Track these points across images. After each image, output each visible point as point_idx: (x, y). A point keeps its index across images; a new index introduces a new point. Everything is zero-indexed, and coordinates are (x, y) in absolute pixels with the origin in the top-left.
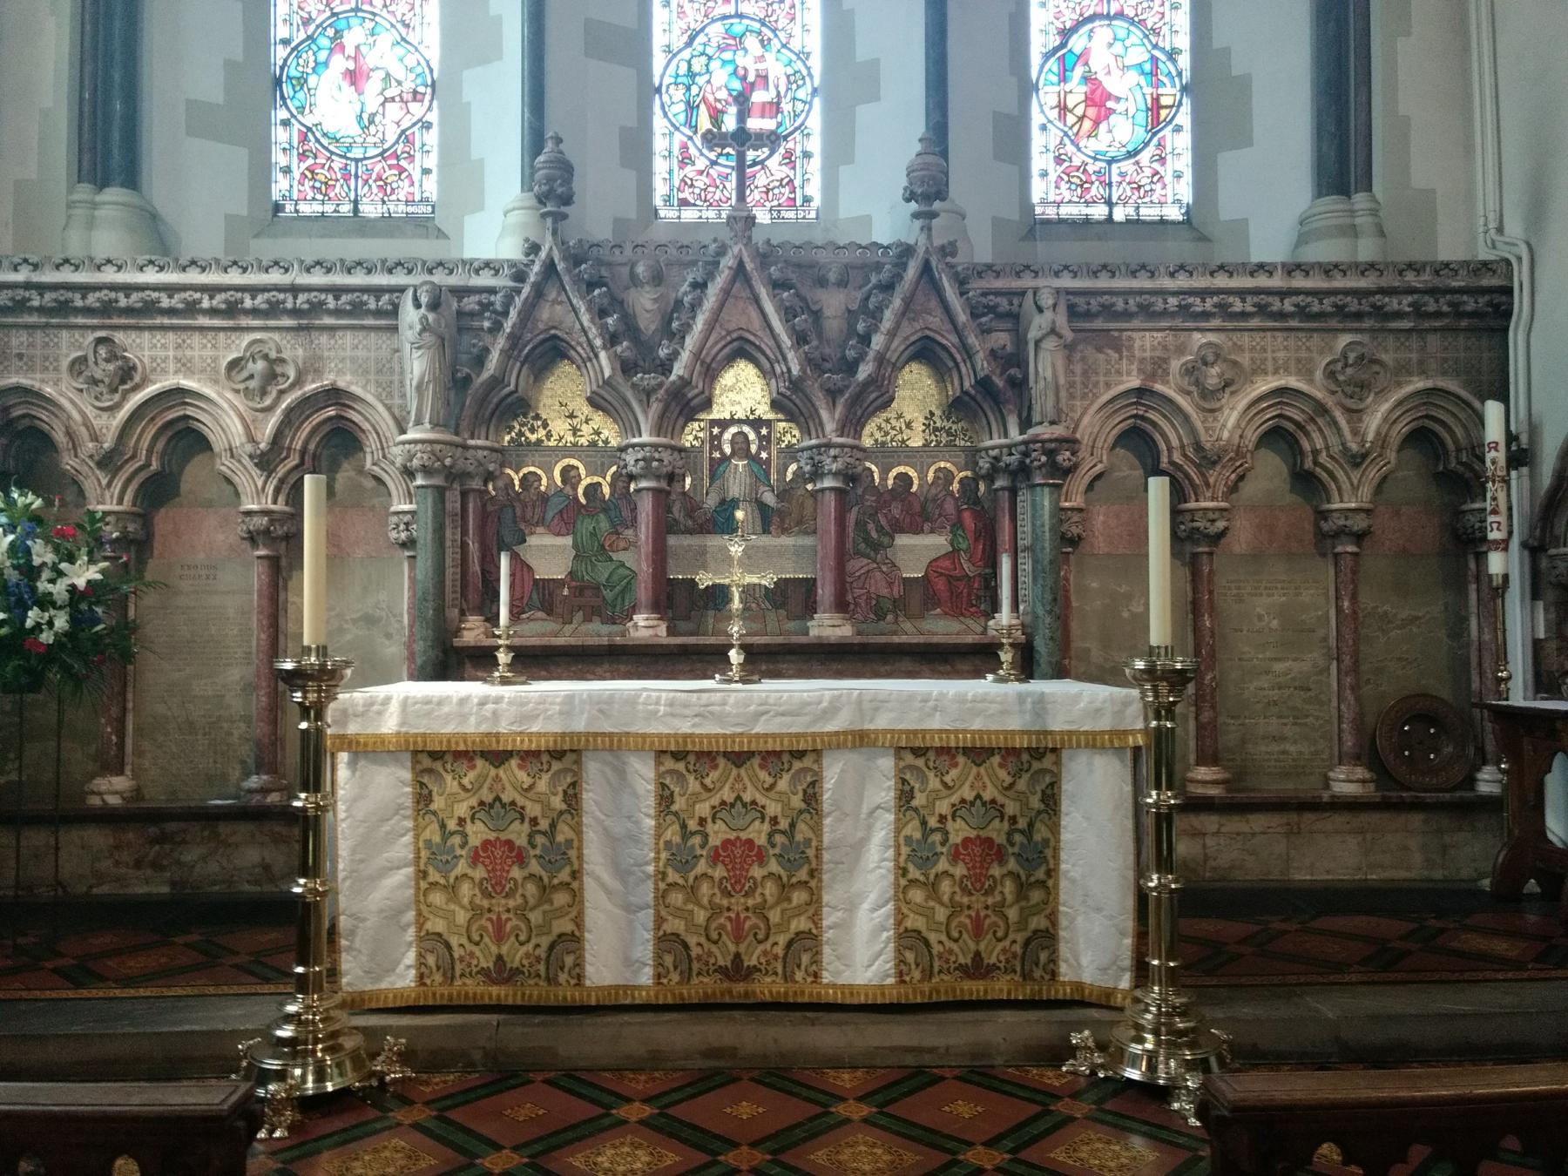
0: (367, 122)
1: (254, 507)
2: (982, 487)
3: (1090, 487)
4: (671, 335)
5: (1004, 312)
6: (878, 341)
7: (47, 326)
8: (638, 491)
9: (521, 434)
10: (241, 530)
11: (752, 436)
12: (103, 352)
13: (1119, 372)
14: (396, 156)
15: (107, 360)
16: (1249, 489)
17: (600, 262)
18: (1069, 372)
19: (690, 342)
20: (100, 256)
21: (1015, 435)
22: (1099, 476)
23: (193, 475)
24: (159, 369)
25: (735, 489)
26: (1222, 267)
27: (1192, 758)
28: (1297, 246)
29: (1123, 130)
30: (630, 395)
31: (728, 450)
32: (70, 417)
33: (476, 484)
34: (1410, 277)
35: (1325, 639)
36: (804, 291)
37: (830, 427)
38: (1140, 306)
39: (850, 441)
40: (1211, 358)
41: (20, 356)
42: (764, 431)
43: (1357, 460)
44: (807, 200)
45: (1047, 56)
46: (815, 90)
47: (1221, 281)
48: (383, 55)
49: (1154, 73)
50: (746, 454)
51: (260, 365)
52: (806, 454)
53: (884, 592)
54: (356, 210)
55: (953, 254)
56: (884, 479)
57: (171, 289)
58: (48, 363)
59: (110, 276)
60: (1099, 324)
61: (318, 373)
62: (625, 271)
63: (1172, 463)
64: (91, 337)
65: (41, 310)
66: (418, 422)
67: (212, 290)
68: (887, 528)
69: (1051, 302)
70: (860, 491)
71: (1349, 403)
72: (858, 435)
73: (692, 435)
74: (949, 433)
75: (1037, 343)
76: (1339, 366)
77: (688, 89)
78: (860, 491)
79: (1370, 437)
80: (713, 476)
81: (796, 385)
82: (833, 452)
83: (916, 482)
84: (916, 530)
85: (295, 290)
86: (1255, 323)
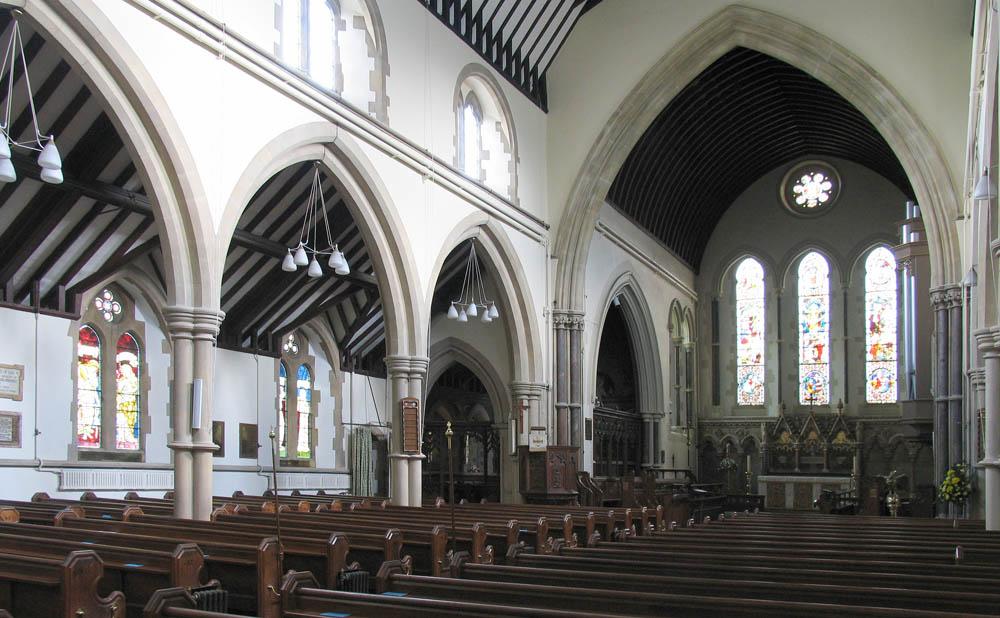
29: (881, 389)
48: (755, 380)
73: (805, 442)
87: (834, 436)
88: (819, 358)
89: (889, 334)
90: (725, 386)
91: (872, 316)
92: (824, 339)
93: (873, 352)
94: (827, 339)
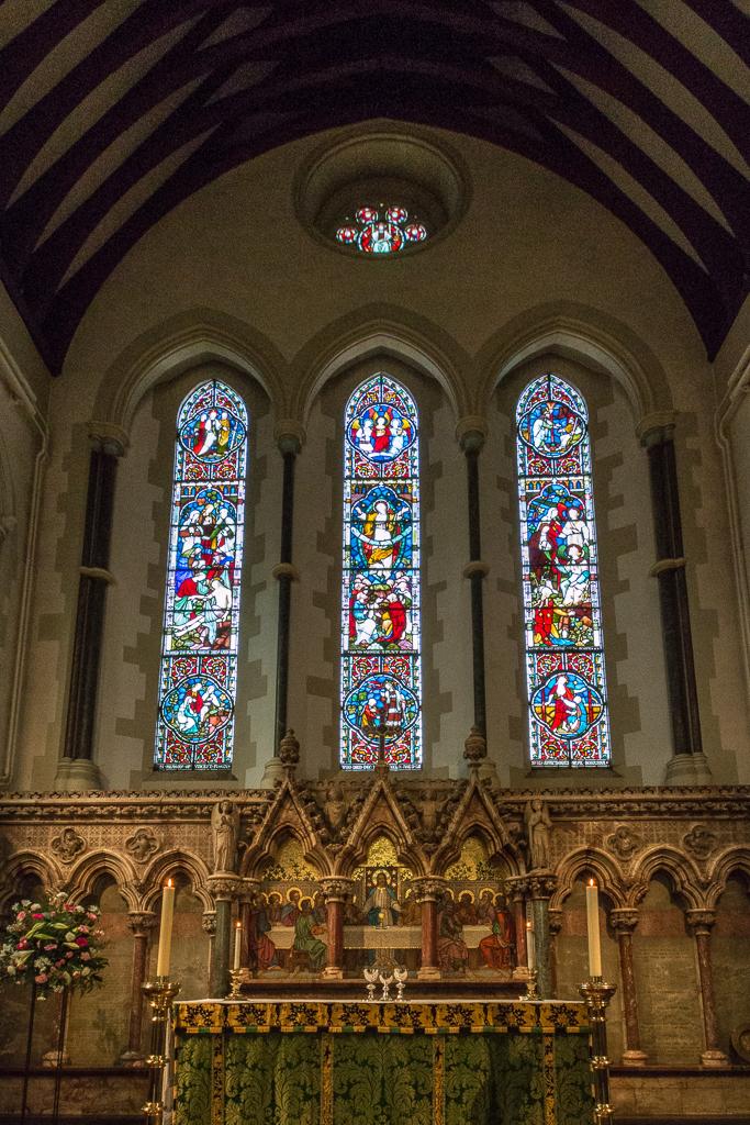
0: (200, 725)
1: (136, 912)
2: (508, 901)
3: (564, 901)
4: (347, 825)
5: (517, 813)
6: (452, 827)
7: (44, 824)
8: (329, 903)
9: (270, 875)
10: (129, 924)
11: (388, 875)
12: (68, 836)
13: (576, 842)
14: (215, 743)
15: (70, 840)
16: (650, 901)
17: (311, 790)
18: (550, 842)
19: (356, 828)
20: (71, 790)
21: (524, 873)
22: (568, 896)
23: (107, 895)
24: (94, 843)
25: (379, 903)
26: (627, 789)
27: (626, 1047)
28: (667, 778)
30: (325, 854)
31: (375, 882)
32: (50, 868)
33: (247, 900)
34: (725, 793)
35: (694, 982)
36: (414, 802)
37: (428, 870)
38: (586, 808)
39: (438, 877)
40: (624, 834)
41: (29, 838)
42: (394, 873)
43: (705, 886)
44: (416, 759)
45: (534, 690)
46: (420, 707)
47: (627, 796)
48: (210, 695)
49: (589, 697)
50: (385, 884)
51: (143, 841)
52: (415, 884)
53: (457, 956)
54: (193, 768)
55: (490, 784)
56: (456, 897)
57: (102, 805)
58: (43, 842)
59: (75, 799)
60: (565, 818)
61: (171, 845)
62: (325, 793)
63: (606, 888)
64: (63, 829)
65: (42, 817)
66: (219, 869)
67: (122, 805)
68: (459, 923)
69: (539, 807)
70: (444, 903)
71: (698, 856)
72: (442, 874)
73: (357, 875)
74: (490, 873)
75: (534, 827)
76: (692, 838)
77: (357, 707)
78: (444, 903)
79: (711, 873)
80: (368, 896)
81: (410, 849)
82: (429, 882)
83: (473, 899)
84: (475, 923)
85: (161, 805)
86: (646, 816)
87: (445, 860)
88: (395, 638)
89: (576, 589)
90: (118, 695)
91: (535, 536)
92: (408, 588)
93: (542, 627)
94: (417, 590)
